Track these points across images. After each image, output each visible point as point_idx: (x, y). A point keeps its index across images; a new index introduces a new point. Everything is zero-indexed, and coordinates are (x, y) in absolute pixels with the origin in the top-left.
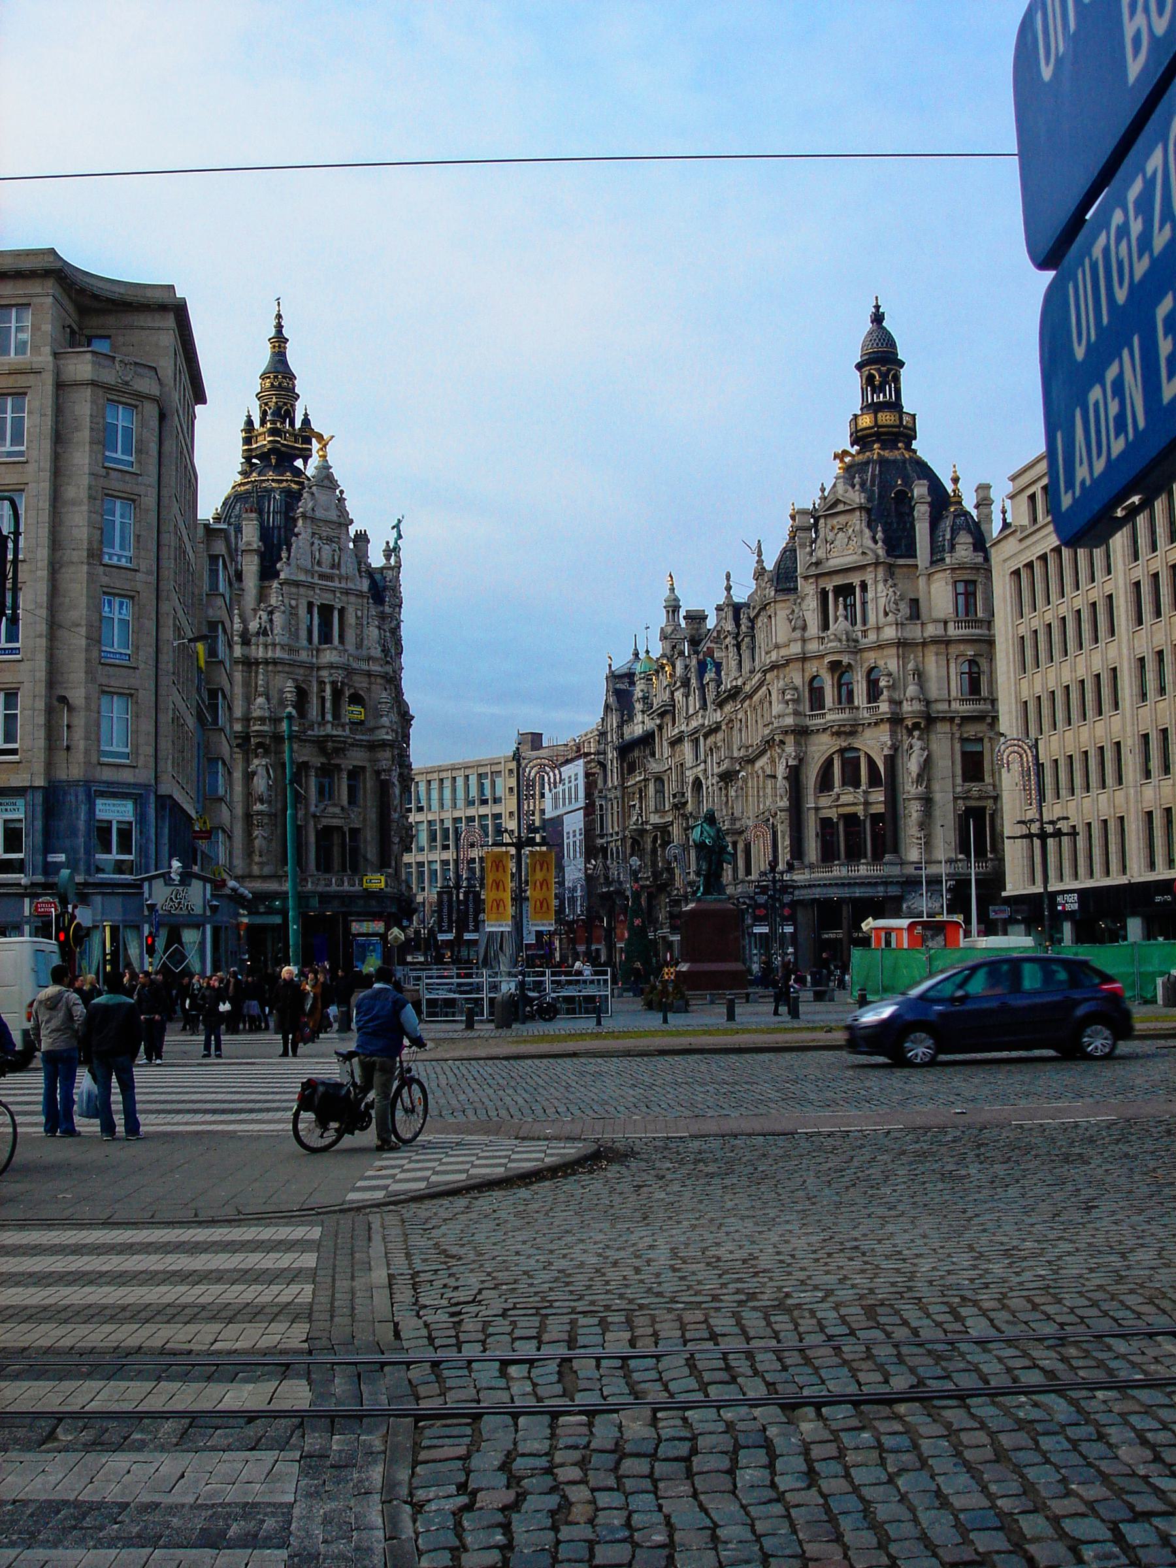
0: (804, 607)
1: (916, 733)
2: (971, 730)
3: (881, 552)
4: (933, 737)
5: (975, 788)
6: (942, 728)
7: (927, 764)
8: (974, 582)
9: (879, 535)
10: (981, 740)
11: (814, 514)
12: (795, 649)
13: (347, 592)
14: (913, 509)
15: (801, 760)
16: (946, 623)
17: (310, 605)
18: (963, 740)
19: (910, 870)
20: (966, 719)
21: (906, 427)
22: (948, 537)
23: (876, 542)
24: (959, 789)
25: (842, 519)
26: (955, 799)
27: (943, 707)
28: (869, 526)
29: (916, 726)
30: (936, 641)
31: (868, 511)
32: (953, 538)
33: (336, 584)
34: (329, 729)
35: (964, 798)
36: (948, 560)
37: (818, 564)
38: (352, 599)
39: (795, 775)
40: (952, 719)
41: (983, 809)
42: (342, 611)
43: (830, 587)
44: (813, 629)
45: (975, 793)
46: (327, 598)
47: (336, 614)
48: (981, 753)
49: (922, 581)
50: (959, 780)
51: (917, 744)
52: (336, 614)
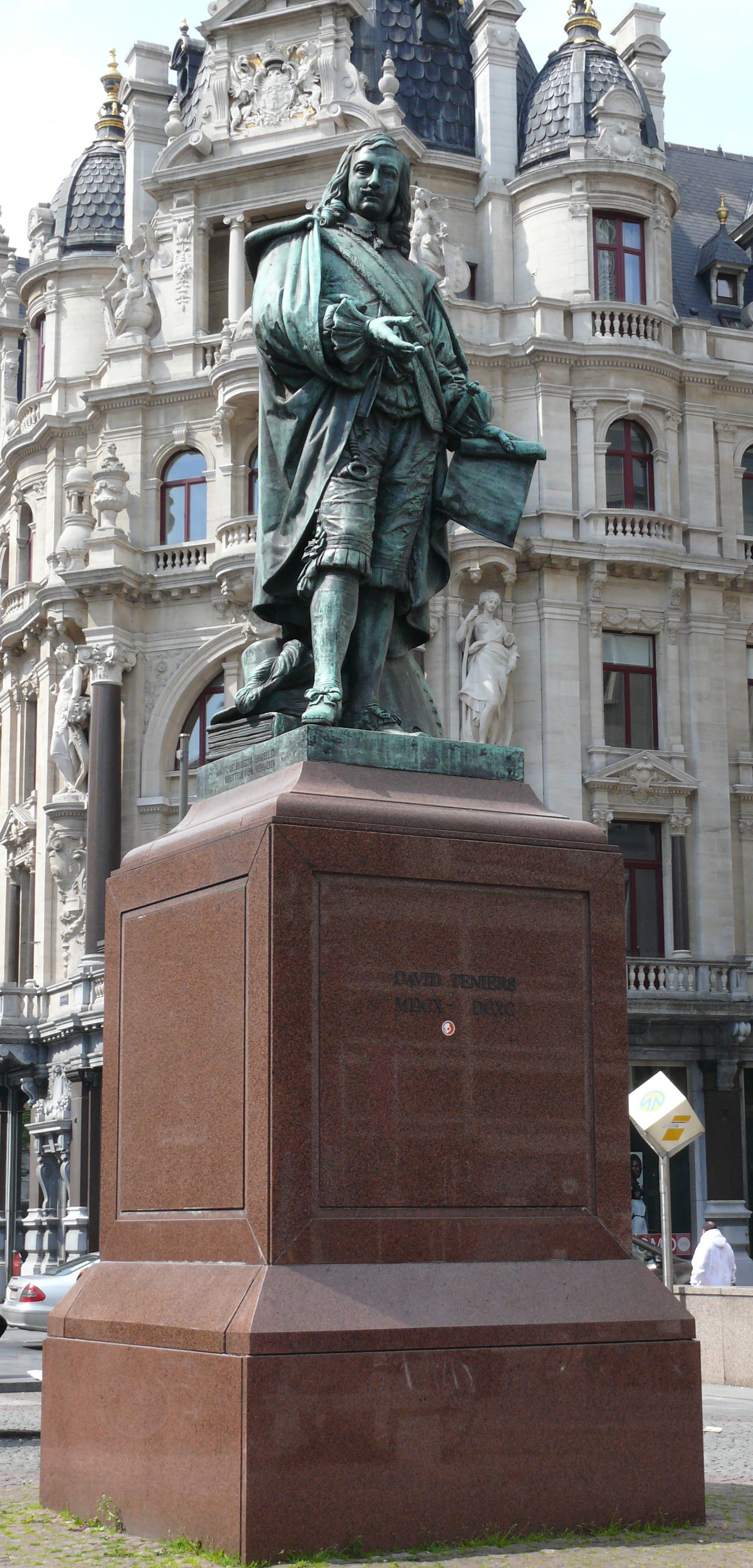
0: (156, 269)
1: (491, 598)
2: (639, 605)
3: (392, 122)
4: (529, 613)
5: (642, 761)
6: (559, 590)
7: (514, 689)
8: (639, 220)
9: (387, 79)
11: (189, 59)
12: (126, 374)
14: (468, 37)
15: (125, 673)
16: (569, 315)
20: (621, 571)
22: (576, 96)
23: (374, 95)
25: (283, 41)
26: (589, 789)
27: (559, 531)
28: (355, 57)
30: (540, 356)
31: (355, 22)
32: (588, 104)
35: (612, 789)
36: (576, 155)
37: (198, 153)
39: (106, 723)
40: (585, 568)
43: (234, 216)
44: (180, 320)
45: (643, 779)
48: (651, 672)
49: (494, 211)
50: (599, 742)
51: (492, 632)
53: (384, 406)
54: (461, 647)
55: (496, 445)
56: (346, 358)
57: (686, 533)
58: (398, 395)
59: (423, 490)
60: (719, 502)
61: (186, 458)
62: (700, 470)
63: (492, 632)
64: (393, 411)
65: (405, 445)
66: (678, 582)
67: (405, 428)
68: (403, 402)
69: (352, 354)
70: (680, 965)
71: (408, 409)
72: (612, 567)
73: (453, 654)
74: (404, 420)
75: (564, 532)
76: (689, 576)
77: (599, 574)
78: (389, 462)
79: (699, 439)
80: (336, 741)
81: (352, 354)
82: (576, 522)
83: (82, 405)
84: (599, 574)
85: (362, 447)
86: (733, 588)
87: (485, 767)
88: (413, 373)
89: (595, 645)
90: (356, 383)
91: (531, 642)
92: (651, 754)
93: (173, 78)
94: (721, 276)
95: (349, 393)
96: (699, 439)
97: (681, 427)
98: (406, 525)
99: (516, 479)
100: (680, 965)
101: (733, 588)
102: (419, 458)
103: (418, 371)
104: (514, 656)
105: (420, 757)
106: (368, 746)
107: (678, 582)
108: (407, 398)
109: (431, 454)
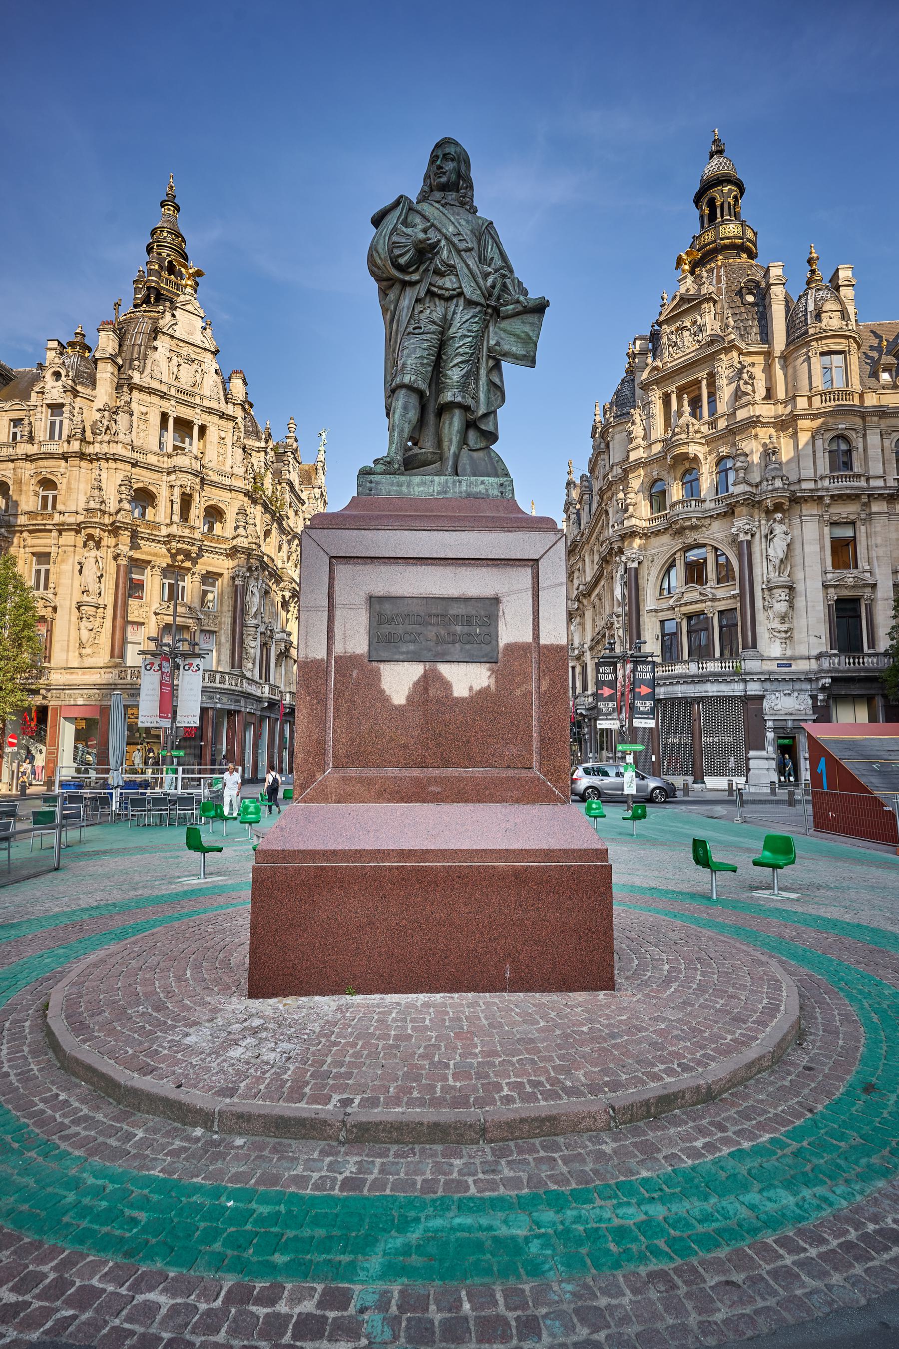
1: (779, 516)
6: (809, 510)
10: (853, 523)
13: (210, 411)
17: (164, 417)
18: (834, 524)
19: (772, 666)
20: (835, 498)
21: (749, 240)
22: (811, 307)
24: (829, 576)
26: (826, 587)
29: (778, 507)
33: (198, 401)
34: (174, 529)
35: (835, 587)
38: (216, 419)
40: (821, 498)
41: (856, 601)
42: (203, 429)
45: (850, 581)
46: (186, 413)
47: (196, 429)
48: (854, 538)
52: (196, 429)
53: (436, 290)
54: (766, 537)
55: (518, 305)
56: (402, 261)
57: (868, 480)
58: (449, 282)
59: (469, 339)
60: (884, 464)
61: (659, 483)
62: (874, 451)
63: (779, 529)
64: (443, 292)
65: (454, 313)
66: (864, 499)
67: (455, 301)
68: (448, 285)
69: (406, 257)
70: (870, 655)
71: (454, 290)
72: (832, 497)
73: (763, 540)
74: (451, 298)
75: (811, 485)
76: (869, 495)
77: (827, 501)
78: (445, 324)
79: (874, 439)
80: (377, 483)
81: (406, 257)
82: (816, 481)
83: (620, 471)
84: (827, 501)
85: (422, 316)
86: (891, 498)
87: (483, 491)
88: (454, 267)
89: (827, 530)
90: (415, 277)
91: (796, 532)
92: (855, 571)
93: (650, 346)
94: (884, 371)
95: (412, 284)
96: (874, 439)
97: (864, 436)
98: (462, 362)
99: (532, 324)
100: (870, 655)
101: (891, 498)
102: (464, 320)
103: (458, 267)
104: (789, 537)
105: (437, 488)
106: (400, 485)
107: (864, 499)
108: (453, 283)
109: (473, 317)
